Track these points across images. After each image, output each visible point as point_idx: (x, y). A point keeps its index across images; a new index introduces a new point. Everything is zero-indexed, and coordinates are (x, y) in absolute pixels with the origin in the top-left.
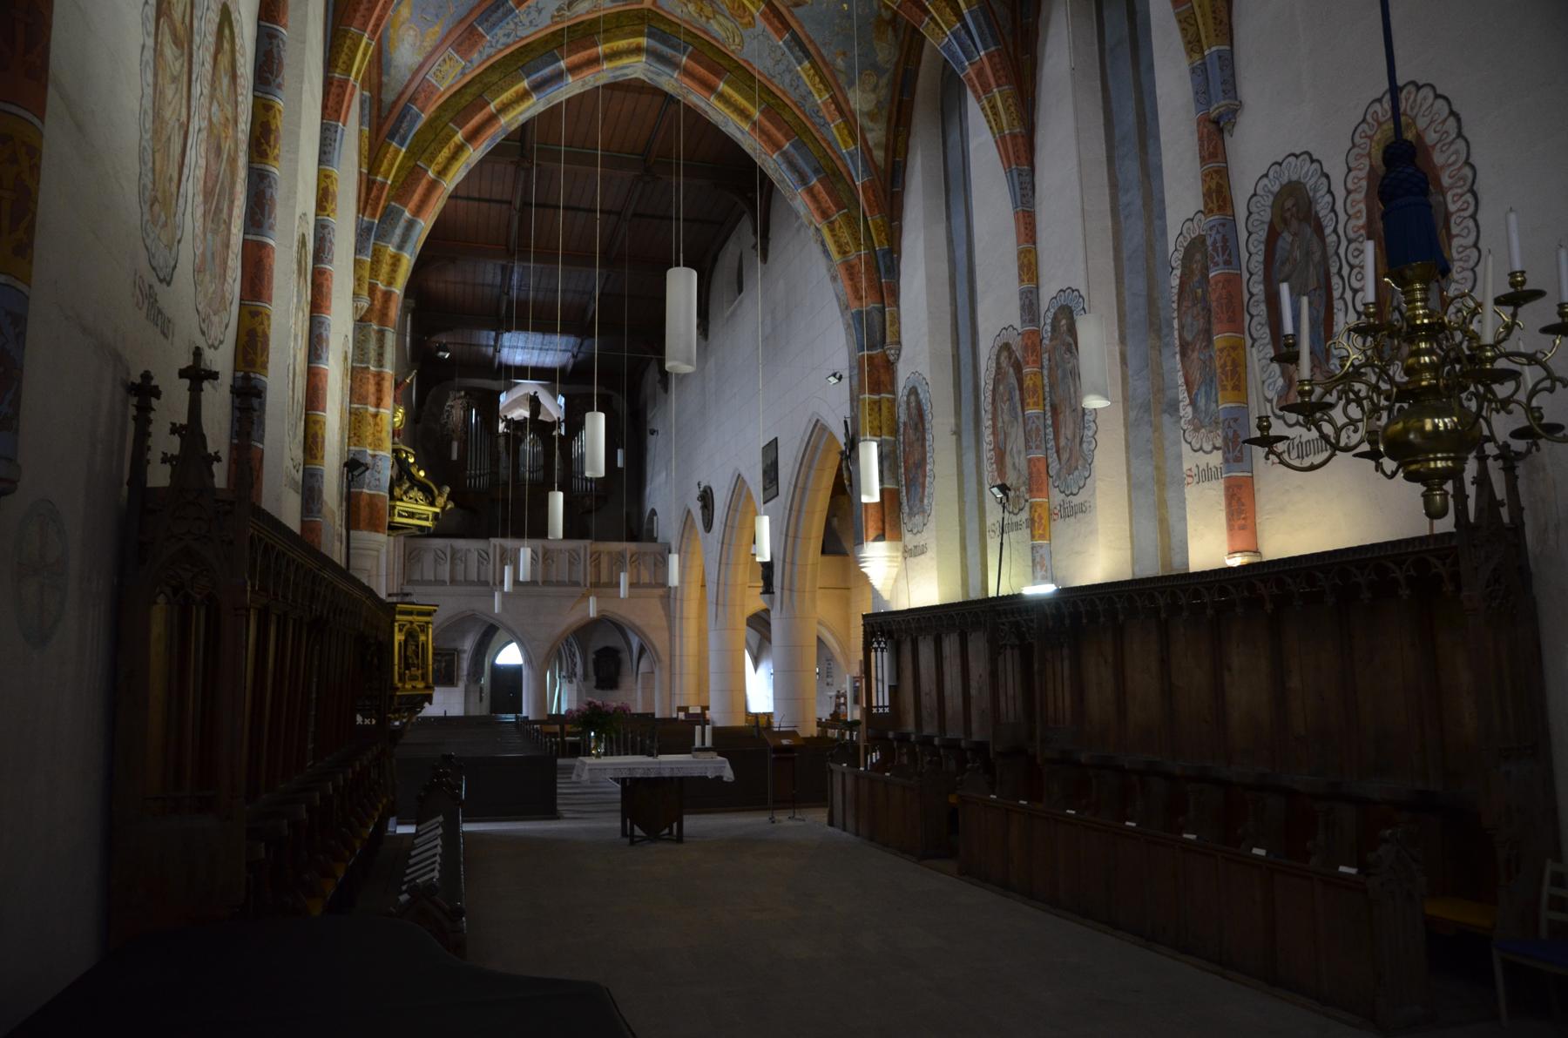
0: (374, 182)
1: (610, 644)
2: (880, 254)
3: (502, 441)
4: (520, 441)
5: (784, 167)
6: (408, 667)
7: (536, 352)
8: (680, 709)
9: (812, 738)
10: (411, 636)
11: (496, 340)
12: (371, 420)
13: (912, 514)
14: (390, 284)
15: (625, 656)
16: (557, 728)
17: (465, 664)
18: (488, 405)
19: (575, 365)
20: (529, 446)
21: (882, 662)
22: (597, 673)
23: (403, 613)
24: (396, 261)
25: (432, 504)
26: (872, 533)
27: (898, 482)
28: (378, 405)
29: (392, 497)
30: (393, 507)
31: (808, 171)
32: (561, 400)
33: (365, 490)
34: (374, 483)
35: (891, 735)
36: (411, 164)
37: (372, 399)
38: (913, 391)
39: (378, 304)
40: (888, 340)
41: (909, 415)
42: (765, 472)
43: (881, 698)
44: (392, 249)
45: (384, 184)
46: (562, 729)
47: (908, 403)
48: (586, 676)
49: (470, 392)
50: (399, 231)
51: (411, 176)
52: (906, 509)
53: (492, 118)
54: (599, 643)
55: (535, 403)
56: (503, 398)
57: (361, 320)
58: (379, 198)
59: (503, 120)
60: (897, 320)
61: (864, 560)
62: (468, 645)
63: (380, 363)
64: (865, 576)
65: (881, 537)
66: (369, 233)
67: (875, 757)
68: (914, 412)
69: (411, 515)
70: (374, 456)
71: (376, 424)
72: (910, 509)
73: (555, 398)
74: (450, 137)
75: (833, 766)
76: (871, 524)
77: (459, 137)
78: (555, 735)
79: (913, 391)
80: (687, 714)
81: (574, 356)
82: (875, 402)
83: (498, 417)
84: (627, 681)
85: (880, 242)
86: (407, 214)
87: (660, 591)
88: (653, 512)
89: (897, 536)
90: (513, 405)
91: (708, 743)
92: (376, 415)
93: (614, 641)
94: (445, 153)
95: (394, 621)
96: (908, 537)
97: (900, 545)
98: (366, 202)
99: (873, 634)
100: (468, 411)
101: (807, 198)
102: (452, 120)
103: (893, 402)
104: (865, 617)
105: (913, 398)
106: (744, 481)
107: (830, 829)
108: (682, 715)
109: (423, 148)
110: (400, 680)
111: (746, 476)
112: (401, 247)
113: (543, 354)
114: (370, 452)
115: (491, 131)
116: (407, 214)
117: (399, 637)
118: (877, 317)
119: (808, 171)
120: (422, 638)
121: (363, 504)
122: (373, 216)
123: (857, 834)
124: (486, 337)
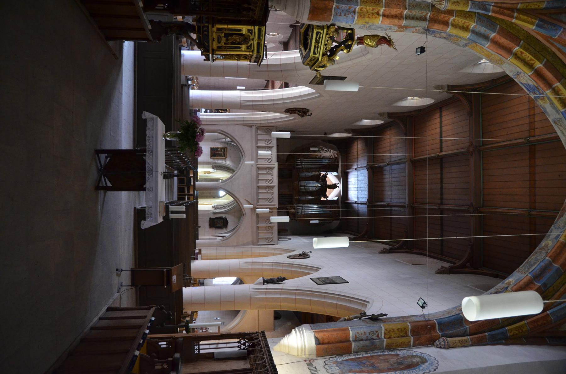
0: (513, 12)
1: (229, 224)
2: (503, 330)
3: (317, 173)
4: (317, 181)
5: (542, 264)
6: (226, 36)
7: (356, 186)
8: (200, 250)
9: (182, 309)
10: (245, 39)
11: (361, 167)
12: (375, 11)
13: (338, 364)
14: (453, 25)
15: (224, 230)
16: (191, 193)
17: (220, 162)
18: (332, 168)
19: (350, 203)
20: (315, 185)
21: (231, 347)
22: (216, 218)
23: (260, 31)
24: (465, 29)
25: (323, 55)
26: (320, 335)
27: (356, 352)
28: (384, 15)
29: (328, 27)
30: (322, 28)
31: (544, 280)
32: (336, 199)
33: (335, 4)
34: (339, 11)
35: (177, 355)
36: (521, 38)
37: (387, 13)
38: (424, 361)
39: (442, 17)
40: (449, 339)
41: (405, 358)
42: (327, 278)
43: (205, 347)
44: (473, 25)
45: (512, 17)
46: (191, 195)
47: (413, 356)
48: (215, 213)
49: (336, 159)
50: (482, 30)
51: (515, 35)
52: (340, 359)
53: (549, 85)
54: (230, 219)
55: (334, 186)
56: (335, 173)
57: (433, 6)
58: (504, 14)
59: (548, 92)
60: (463, 345)
61: (301, 332)
62: (228, 163)
63: (408, 18)
64: (289, 332)
65: (318, 342)
66: (482, 10)
67: (163, 344)
68: (409, 361)
69: (317, 41)
70: (354, 12)
71: (373, 14)
72: (341, 363)
73: (336, 197)
74: (538, 60)
75: (153, 310)
76: (327, 334)
77: (538, 65)
78: (188, 191)
79: (424, 361)
80: (198, 254)
81: (356, 203)
82: (406, 333)
83: (327, 171)
84: (214, 231)
85: (511, 330)
86: (493, 35)
87: (255, 241)
88: (290, 239)
89: (320, 354)
90: (332, 178)
91: (172, 216)
92: (378, 14)
93: (231, 226)
94: (528, 56)
95: (255, 25)
96: (319, 363)
97: (314, 357)
98: (500, 7)
99: (251, 339)
100: (330, 158)
101: (525, 280)
102: (548, 60)
103: (407, 345)
104: (263, 333)
105: (418, 360)
106: (317, 271)
107: (105, 309)
108: (197, 251)
109: (531, 43)
110: (219, 30)
111: (320, 271)
112: (473, 32)
113: (356, 189)
114: (358, 8)
115: (541, 85)
116: (493, 35)
117: (244, 29)
118: (460, 330)
119: (544, 280)
120: (244, 47)
121: (327, 2)
122: (494, 12)
123: (92, 328)
124: (363, 162)
